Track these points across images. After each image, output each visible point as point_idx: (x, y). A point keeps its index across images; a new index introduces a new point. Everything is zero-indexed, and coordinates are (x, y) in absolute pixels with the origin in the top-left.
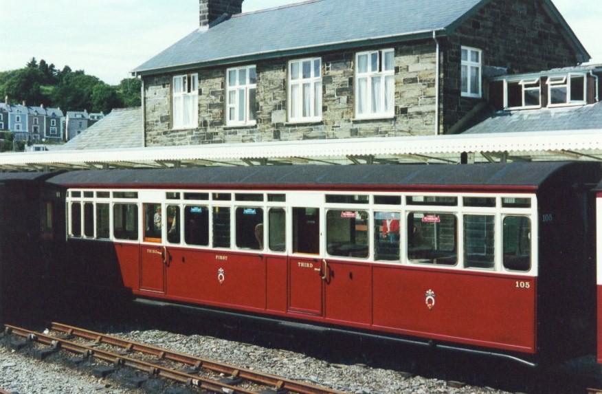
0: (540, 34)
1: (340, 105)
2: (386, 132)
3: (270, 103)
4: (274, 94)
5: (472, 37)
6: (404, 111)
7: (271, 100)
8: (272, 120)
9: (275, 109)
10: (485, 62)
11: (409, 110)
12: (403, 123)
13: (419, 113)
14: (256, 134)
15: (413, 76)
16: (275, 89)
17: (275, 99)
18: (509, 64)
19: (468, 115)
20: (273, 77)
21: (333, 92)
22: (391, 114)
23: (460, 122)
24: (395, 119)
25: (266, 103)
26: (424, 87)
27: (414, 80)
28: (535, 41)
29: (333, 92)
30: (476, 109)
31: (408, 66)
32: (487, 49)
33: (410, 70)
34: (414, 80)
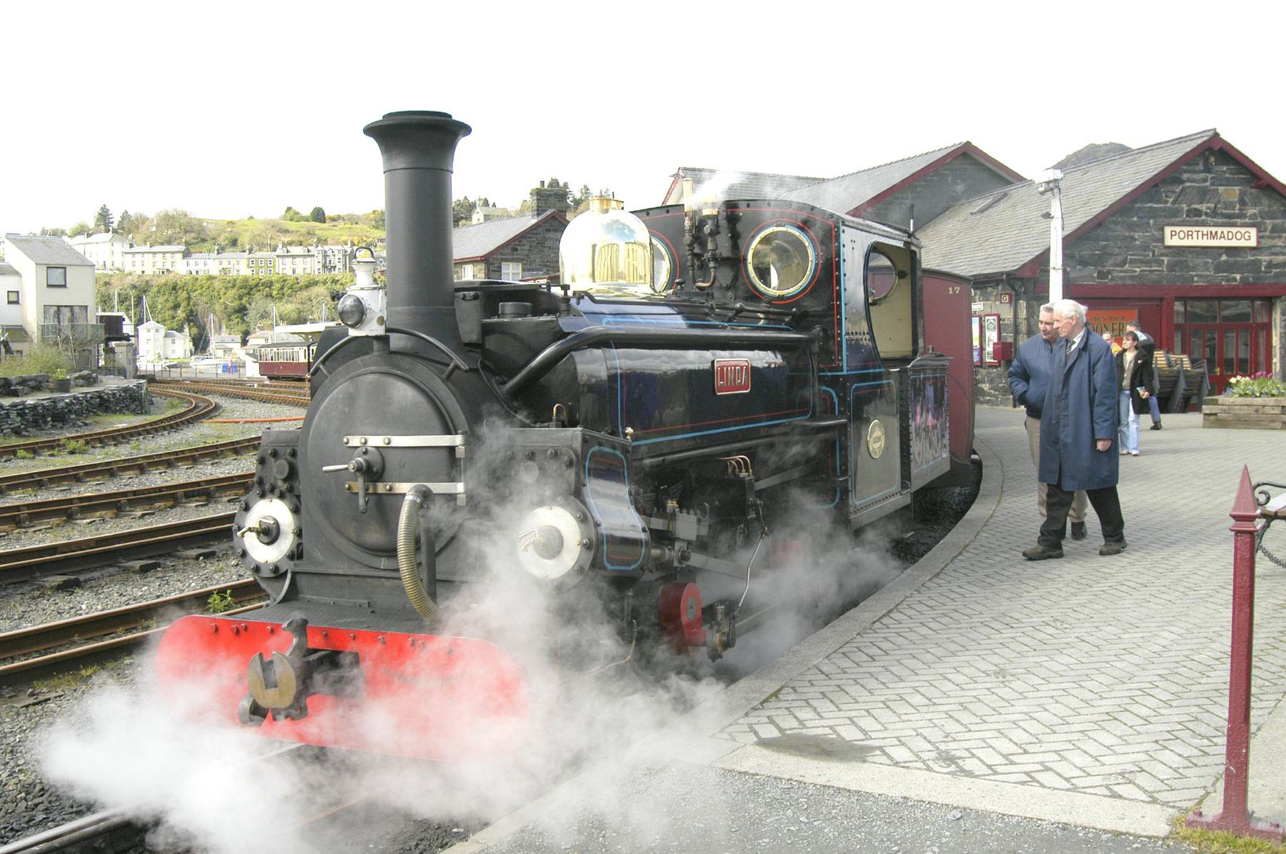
5: (510, 257)
10: (523, 270)
18: (545, 270)
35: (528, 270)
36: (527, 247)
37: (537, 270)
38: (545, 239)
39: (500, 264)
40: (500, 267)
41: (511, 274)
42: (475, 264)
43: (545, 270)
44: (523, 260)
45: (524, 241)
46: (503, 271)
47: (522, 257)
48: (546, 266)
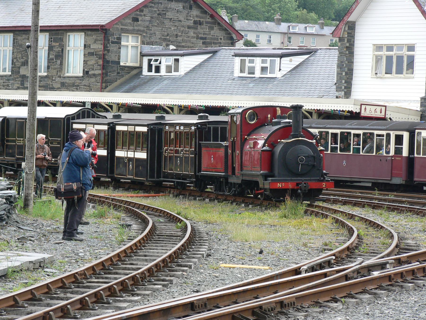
0: (195, 22)
1: (56, 67)
2: (78, 86)
3: (20, 61)
4: (22, 54)
5: (131, 28)
6: (87, 72)
7: (20, 59)
8: (20, 73)
9: (22, 65)
10: (143, 43)
11: (90, 73)
12: (86, 82)
13: (94, 75)
14: (11, 82)
15: (92, 51)
16: (23, 51)
17: (22, 58)
18: (164, 44)
19: (127, 77)
20: (22, 43)
21: (53, 57)
22: (81, 75)
23: (119, 82)
24: (83, 77)
25: (17, 60)
26: (97, 59)
27: (91, 54)
28: (189, 27)
29: (53, 57)
30: (135, 72)
31: (90, 45)
32: (145, 34)
33: (92, 47)
34: (91, 54)
35: (148, 44)
36: (148, 18)
37: (156, 43)
38: (166, 9)
39: (120, 35)
40: (119, 39)
41: (130, 47)
42: (89, 33)
43: (164, 44)
44: (143, 31)
45: (146, 11)
46: (123, 43)
47: (142, 29)
48: (165, 40)
